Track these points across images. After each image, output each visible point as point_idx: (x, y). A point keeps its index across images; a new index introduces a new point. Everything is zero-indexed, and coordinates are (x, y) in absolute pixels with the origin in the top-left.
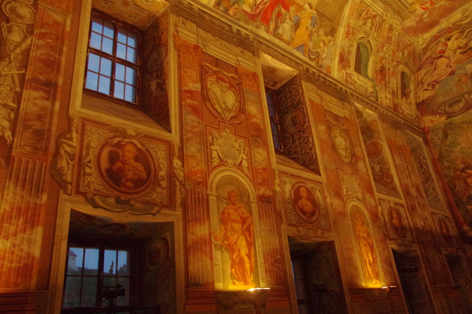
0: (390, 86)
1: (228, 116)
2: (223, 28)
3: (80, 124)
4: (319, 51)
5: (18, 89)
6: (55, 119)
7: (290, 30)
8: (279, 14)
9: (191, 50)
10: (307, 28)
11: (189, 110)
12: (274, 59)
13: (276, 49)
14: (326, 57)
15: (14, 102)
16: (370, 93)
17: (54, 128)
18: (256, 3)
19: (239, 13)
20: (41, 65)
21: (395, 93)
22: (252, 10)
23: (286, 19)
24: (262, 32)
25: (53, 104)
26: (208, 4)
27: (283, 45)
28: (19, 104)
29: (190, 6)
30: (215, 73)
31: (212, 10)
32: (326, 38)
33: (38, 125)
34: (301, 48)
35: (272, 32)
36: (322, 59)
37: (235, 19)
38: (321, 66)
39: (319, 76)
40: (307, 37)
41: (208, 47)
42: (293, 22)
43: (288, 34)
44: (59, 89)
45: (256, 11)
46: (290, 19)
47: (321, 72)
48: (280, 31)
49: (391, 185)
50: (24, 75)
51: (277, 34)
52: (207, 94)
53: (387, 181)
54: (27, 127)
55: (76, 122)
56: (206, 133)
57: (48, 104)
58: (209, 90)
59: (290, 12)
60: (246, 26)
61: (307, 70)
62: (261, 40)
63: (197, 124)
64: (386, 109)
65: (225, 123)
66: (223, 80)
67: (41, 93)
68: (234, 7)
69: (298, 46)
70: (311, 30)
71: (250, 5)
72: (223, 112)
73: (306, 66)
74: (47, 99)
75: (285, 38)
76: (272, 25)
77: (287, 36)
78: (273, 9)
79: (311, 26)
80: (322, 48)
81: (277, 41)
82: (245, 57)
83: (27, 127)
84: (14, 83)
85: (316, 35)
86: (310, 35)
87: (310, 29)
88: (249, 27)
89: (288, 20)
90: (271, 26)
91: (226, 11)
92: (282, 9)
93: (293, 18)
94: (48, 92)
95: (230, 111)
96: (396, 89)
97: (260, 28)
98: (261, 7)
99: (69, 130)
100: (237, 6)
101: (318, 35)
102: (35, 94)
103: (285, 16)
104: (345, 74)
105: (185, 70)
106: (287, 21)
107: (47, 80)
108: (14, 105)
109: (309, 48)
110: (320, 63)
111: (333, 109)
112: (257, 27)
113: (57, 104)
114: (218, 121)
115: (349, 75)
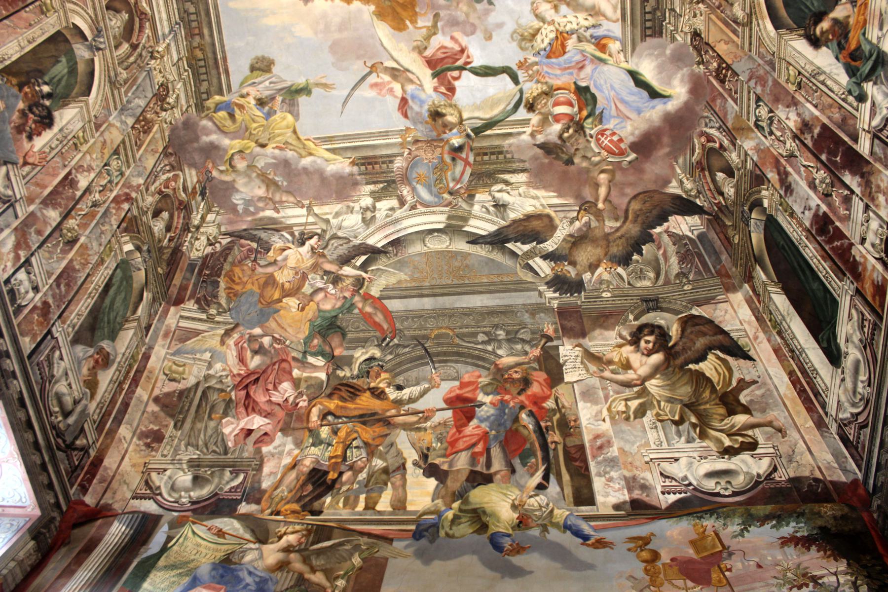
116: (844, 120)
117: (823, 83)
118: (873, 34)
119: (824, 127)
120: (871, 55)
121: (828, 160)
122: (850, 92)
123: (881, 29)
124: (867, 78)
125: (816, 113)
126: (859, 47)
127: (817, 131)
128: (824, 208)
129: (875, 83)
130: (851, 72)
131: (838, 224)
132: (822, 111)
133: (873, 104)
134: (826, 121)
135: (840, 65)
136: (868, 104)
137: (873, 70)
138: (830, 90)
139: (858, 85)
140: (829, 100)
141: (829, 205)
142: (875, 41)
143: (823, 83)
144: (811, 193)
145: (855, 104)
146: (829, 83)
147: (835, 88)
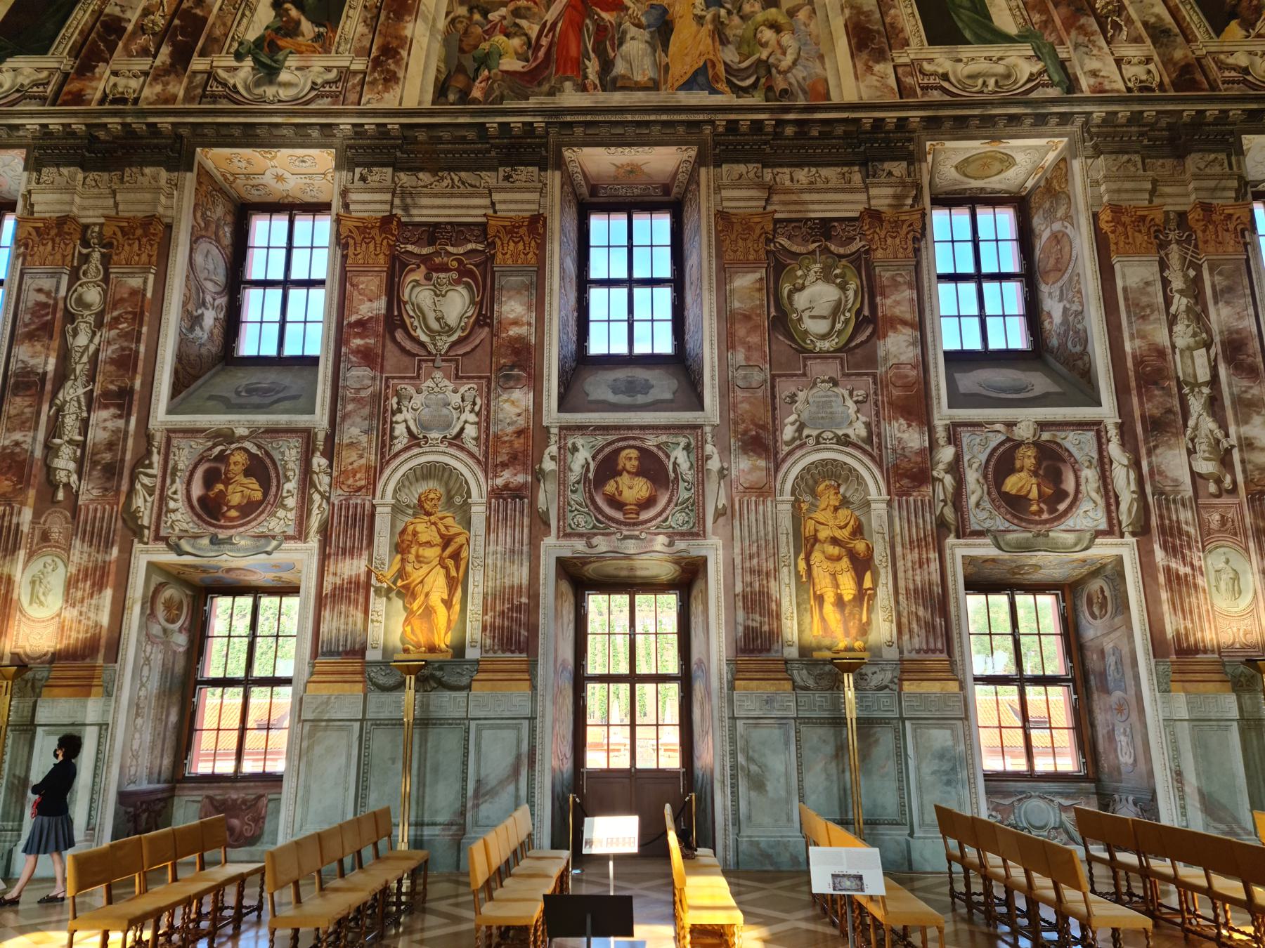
0: (1129, 21)
1: (444, 343)
2: (463, 140)
3: (164, 440)
4: (764, 57)
5: (85, 415)
6: (130, 442)
7: (649, 50)
8: (602, 30)
9: (375, 232)
10: (700, 19)
11: (354, 359)
12: (613, 149)
13: (619, 118)
14: (795, 63)
15: (80, 434)
16: (1029, 81)
17: (128, 456)
18: (529, 39)
19: (496, 85)
20: (113, 368)
21: (1167, 32)
22: (527, 61)
23: (624, 33)
24: (570, 98)
25: (128, 422)
26: (420, 103)
27: (638, 98)
28: (86, 436)
29: (382, 129)
30: (425, 259)
31: (430, 113)
32: (773, 10)
33: (107, 457)
34: (701, 79)
35: (597, 82)
36: (785, 73)
37: (491, 103)
38: (785, 92)
39: (780, 123)
40: (709, 41)
41: (416, 206)
42: (649, 26)
43: (648, 62)
44: (136, 397)
45: (536, 58)
46: (639, 26)
47: (787, 109)
48: (620, 68)
49: (1080, 363)
50: (92, 391)
51: (615, 80)
52: (400, 314)
53: (1074, 350)
54: (94, 463)
55: (159, 438)
56: (386, 395)
57: (121, 423)
58: (405, 303)
59: (627, 8)
60: (523, 105)
61: (732, 126)
62: (569, 119)
63: (369, 382)
64: (1141, 100)
65: (433, 361)
66: (444, 268)
67: (112, 411)
68: (480, 78)
69: (686, 78)
70: (717, 17)
71: (516, 53)
72: (433, 339)
73: (721, 119)
74: (120, 417)
75: (638, 77)
76: (592, 67)
77: (644, 70)
78: (579, 28)
79: (708, 7)
80: (773, 42)
81: (617, 98)
82: (517, 184)
83: (94, 463)
84: (80, 408)
85: (736, 20)
86: (720, 34)
87: (709, 17)
88: (533, 102)
89: (633, 31)
90: (589, 71)
91: (464, 96)
92: (604, 15)
93: (643, 20)
94: (120, 407)
95: (450, 330)
96: (1168, 18)
97: (561, 90)
98: (544, 42)
99: (149, 453)
100: (486, 72)
101: (741, 17)
102: (105, 414)
103: (620, 24)
104: (891, 71)
105: (355, 280)
106: (628, 36)
107: (120, 387)
108: (81, 438)
109: (725, 63)
110: (780, 84)
111: (811, 207)
112: (551, 93)
113: (133, 420)
114: (419, 360)
115: (915, 67)
116: (216, 40)
117: (243, 15)
118: (292, 62)
119: (205, 20)
120: (275, 61)
121: (176, 27)
122: (241, 44)
123: (298, 69)
124: (256, 60)
125: (215, 10)
126: (280, 49)
127: (198, 12)
128: (130, 27)
129: (253, 69)
130: (259, 42)
131: (121, 44)
132: (218, 16)
133: (236, 69)
134: (211, 20)
135: (262, 31)
136: (235, 64)
137: (263, 65)
138: (239, 23)
139: (249, 52)
140: (229, 23)
141: (134, 33)
142: (287, 64)
143: (243, 15)
144: (139, 12)
145: (232, 50)
146: (245, 21)
147: (242, 28)
